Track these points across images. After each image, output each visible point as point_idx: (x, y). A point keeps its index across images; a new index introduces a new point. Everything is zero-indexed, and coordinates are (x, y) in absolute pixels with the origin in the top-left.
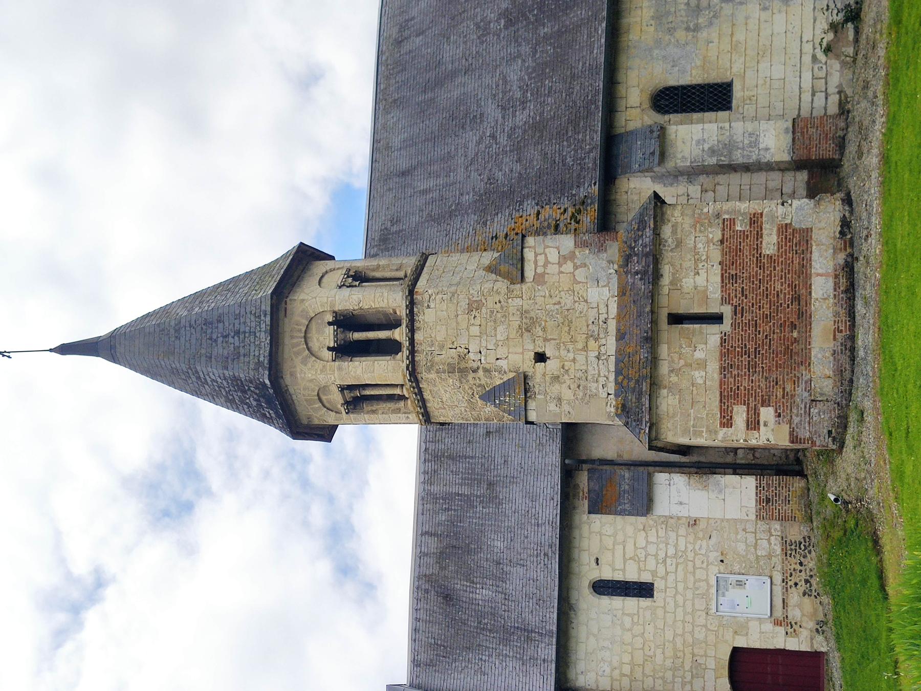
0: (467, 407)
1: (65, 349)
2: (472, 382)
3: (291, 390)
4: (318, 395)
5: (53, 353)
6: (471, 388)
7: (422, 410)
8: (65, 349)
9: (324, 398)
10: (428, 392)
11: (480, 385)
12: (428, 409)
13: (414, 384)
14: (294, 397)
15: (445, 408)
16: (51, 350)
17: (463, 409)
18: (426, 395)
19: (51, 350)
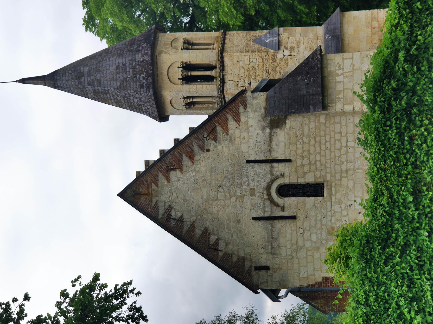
0: (245, 46)
1: (24, 81)
2: (252, 35)
3: (160, 39)
4: (172, 42)
5: (18, 83)
6: (250, 38)
7: (221, 48)
8: (24, 81)
9: (173, 44)
10: (229, 39)
11: (255, 36)
12: (225, 47)
13: (223, 36)
14: (159, 42)
15: (233, 47)
16: (16, 81)
17: (242, 47)
18: (227, 41)
19: (16, 81)
